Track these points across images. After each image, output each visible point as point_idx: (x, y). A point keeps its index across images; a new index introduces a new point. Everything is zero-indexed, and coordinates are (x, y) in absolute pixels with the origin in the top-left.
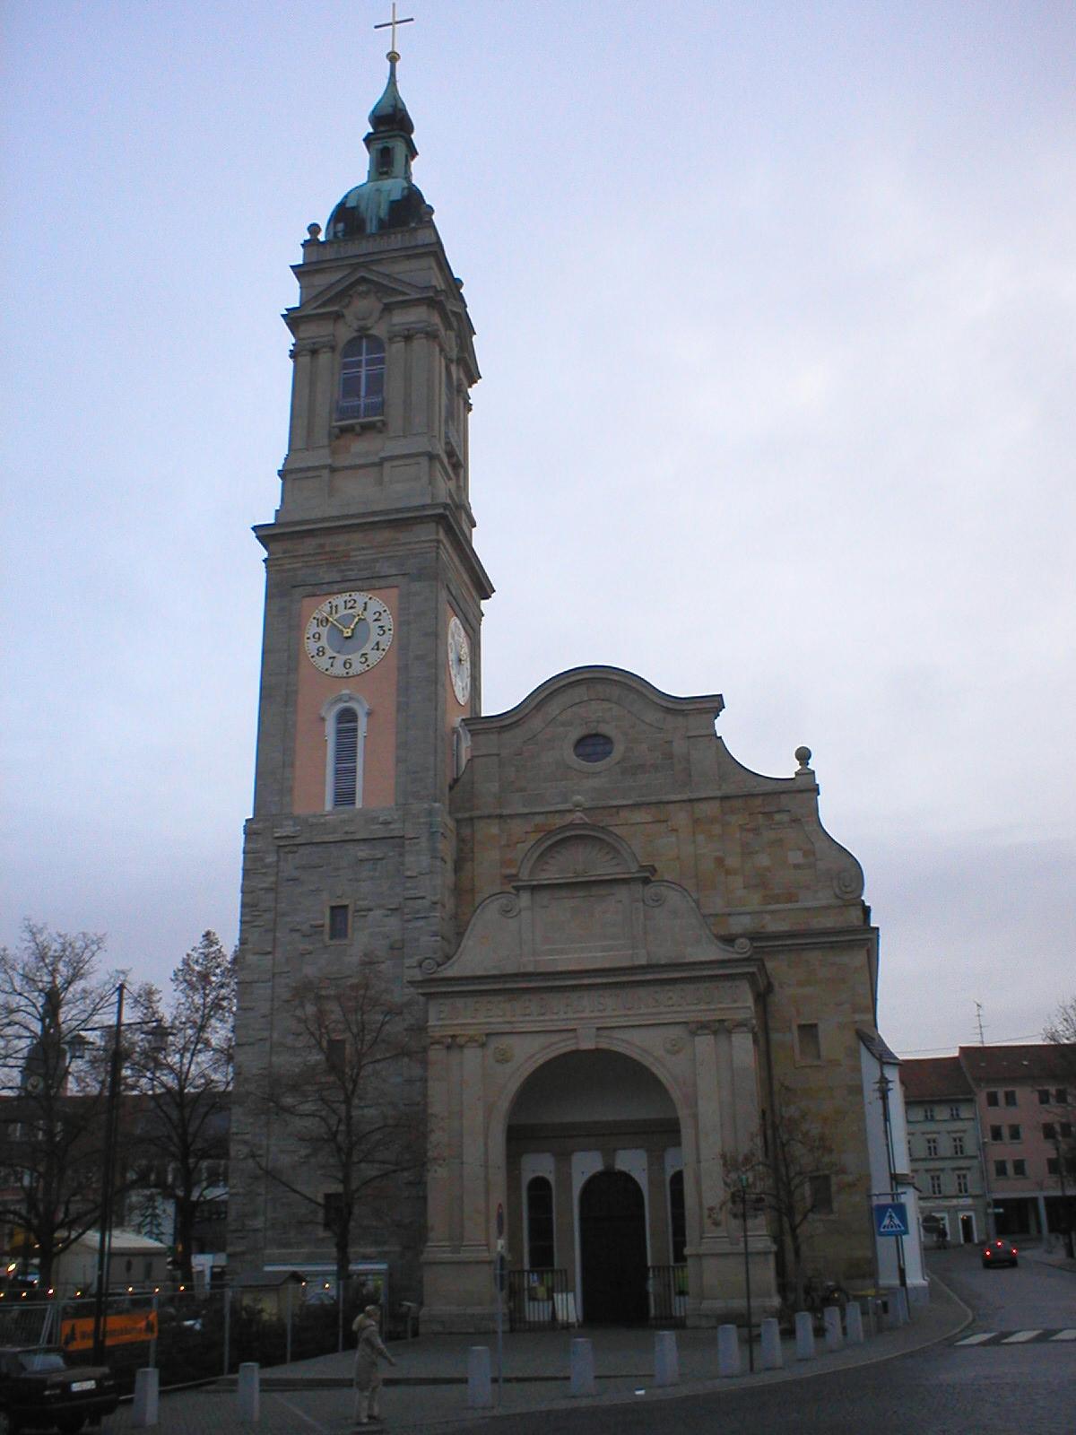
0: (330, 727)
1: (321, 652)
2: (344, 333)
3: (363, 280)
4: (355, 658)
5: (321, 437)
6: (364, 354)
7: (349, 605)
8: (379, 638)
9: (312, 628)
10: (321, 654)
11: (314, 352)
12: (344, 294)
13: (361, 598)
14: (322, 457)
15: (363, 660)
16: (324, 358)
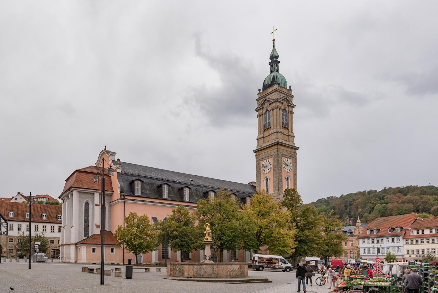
2: (264, 111)
3: (266, 100)
5: (262, 132)
13: (268, 160)
14: (262, 136)
16: (261, 117)
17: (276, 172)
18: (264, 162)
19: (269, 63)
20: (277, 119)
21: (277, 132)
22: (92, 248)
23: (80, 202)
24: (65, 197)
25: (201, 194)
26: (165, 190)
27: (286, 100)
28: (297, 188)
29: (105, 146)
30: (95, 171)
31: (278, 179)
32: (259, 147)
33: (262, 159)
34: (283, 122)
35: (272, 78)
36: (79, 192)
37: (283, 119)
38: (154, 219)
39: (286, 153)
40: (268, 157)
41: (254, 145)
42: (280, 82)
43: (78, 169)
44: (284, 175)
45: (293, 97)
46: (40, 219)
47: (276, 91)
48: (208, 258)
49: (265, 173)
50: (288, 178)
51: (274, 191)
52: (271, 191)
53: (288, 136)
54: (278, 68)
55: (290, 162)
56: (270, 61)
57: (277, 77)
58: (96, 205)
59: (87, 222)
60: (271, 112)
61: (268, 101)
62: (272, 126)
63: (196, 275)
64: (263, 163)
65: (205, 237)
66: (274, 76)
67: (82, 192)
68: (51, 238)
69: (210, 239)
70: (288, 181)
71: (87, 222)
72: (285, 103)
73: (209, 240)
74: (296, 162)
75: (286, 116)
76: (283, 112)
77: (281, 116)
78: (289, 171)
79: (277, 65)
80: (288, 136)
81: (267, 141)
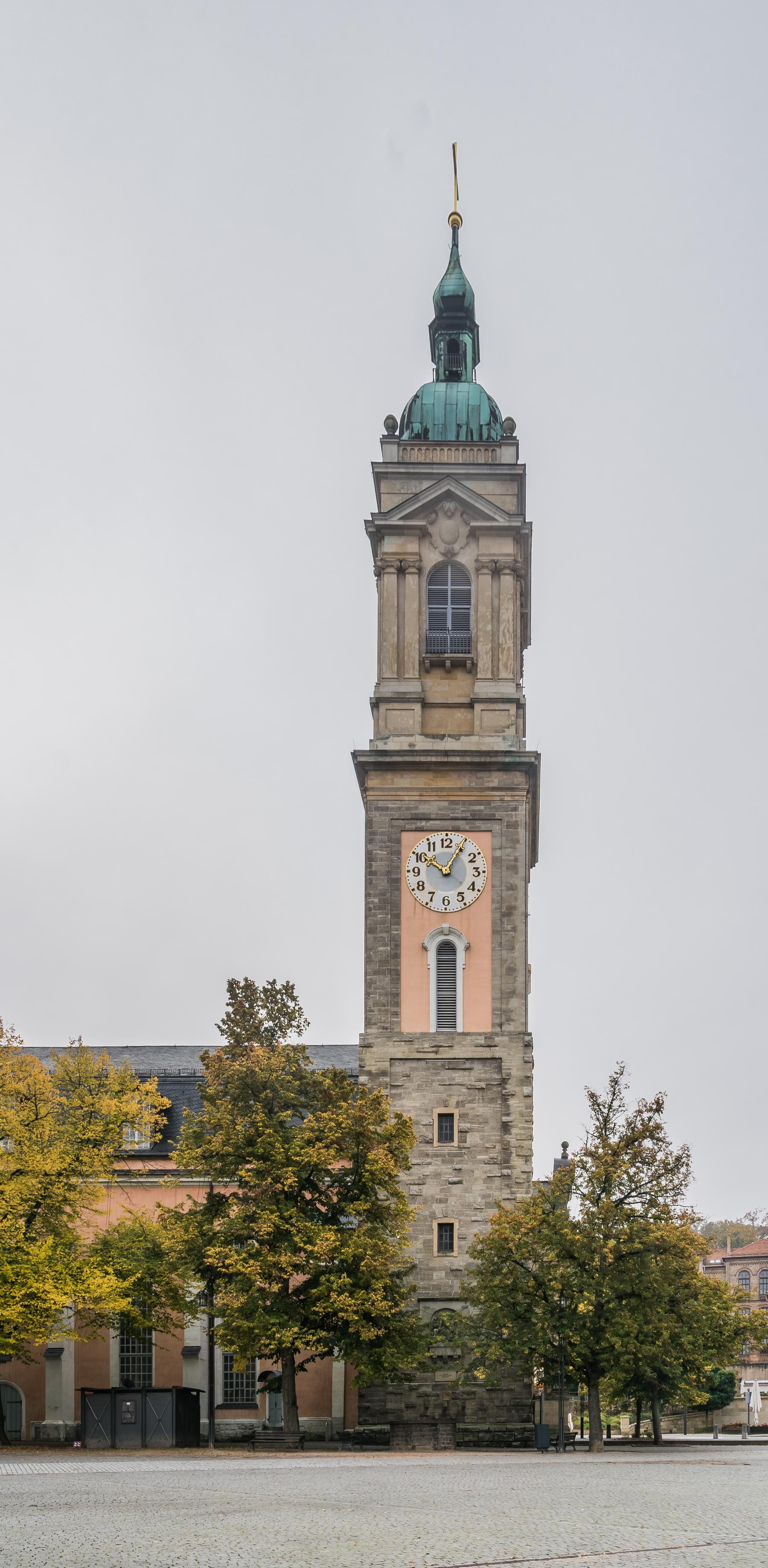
0: (432, 957)
1: (421, 886)
4: (452, 895)
5: (412, 669)
6: (449, 584)
7: (446, 844)
8: (474, 879)
9: (410, 862)
10: (421, 888)
13: (457, 838)
15: (460, 898)
16: (411, 581)
18: (431, 846)
64: (422, 848)
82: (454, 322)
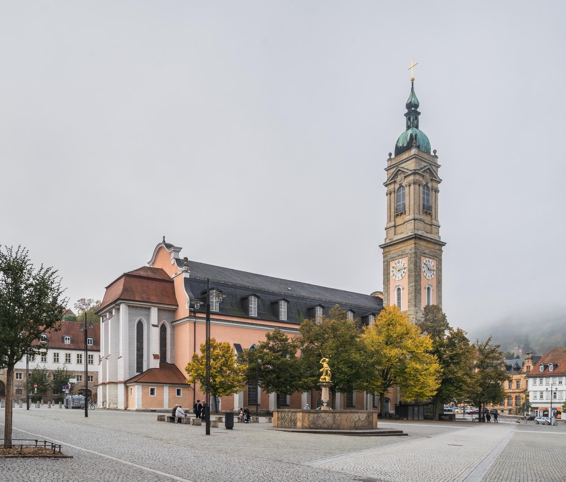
1: (394, 275)
2: (397, 186)
3: (399, 170)
4: (400, 276)
5: (393, 218)
9: (391, 269)
11: (390, 194)
12: (396, 175)
13: (400, 260)
14: (392, 223)
16: (392, 195)
17: (413, 279)
18: (396, 264)
19: (406, 115)
20: (414, 199)
21: (415, 219)
22: (150, 388)
23: (130, 321)
24: (106, 312)
25: (304, 309)
26: (253, 304)
27: (428, 171)
28: (441, 303)
29: (164, 237)
30: (150, 274)
31: (416, 289)
32: (388, 241)
33: (393, 259)
34: (424, 205)
35: (408, 138)
36: (129, 306)
37: (424, 199)
38: (238, 347)
39: (427, 251)
40: (401, 256)
41: (382, 238)
42: (421, 143)
43: (126, 272)
44: (424, 284)
45: (438, 166)
46: (61, 343)
47: (415, 157)
48: (325, 404)
49: (397, 279)
50: (429, 289)
51: (409, 307)
52: (404, 307)
53: (431, 225)
54: (418, 122)
55: (433, 264)
56: (406, 111)
57: (416, 135)
58: (154, 326)
59: (140, 349)
60: (407, 189)
61: (403, 172)
62: (407, 209)
63: (312, 426)
64: (394, 265)
65: (322, 377)
66: (411, 135)
67: (133, 307)
68: (77, 372)
69: (328, 379)
70: (429, 293)
71: (140, 349)
72: (427, 176)
73: (327, 380)
74: (441, 264)
75: (428, 195)
76: (424, 189)
77: (421, 195)
78: (430, 278)
79: (417, 118)
80: (431, 225)
81: (400, 232)
82: (413, 112)
